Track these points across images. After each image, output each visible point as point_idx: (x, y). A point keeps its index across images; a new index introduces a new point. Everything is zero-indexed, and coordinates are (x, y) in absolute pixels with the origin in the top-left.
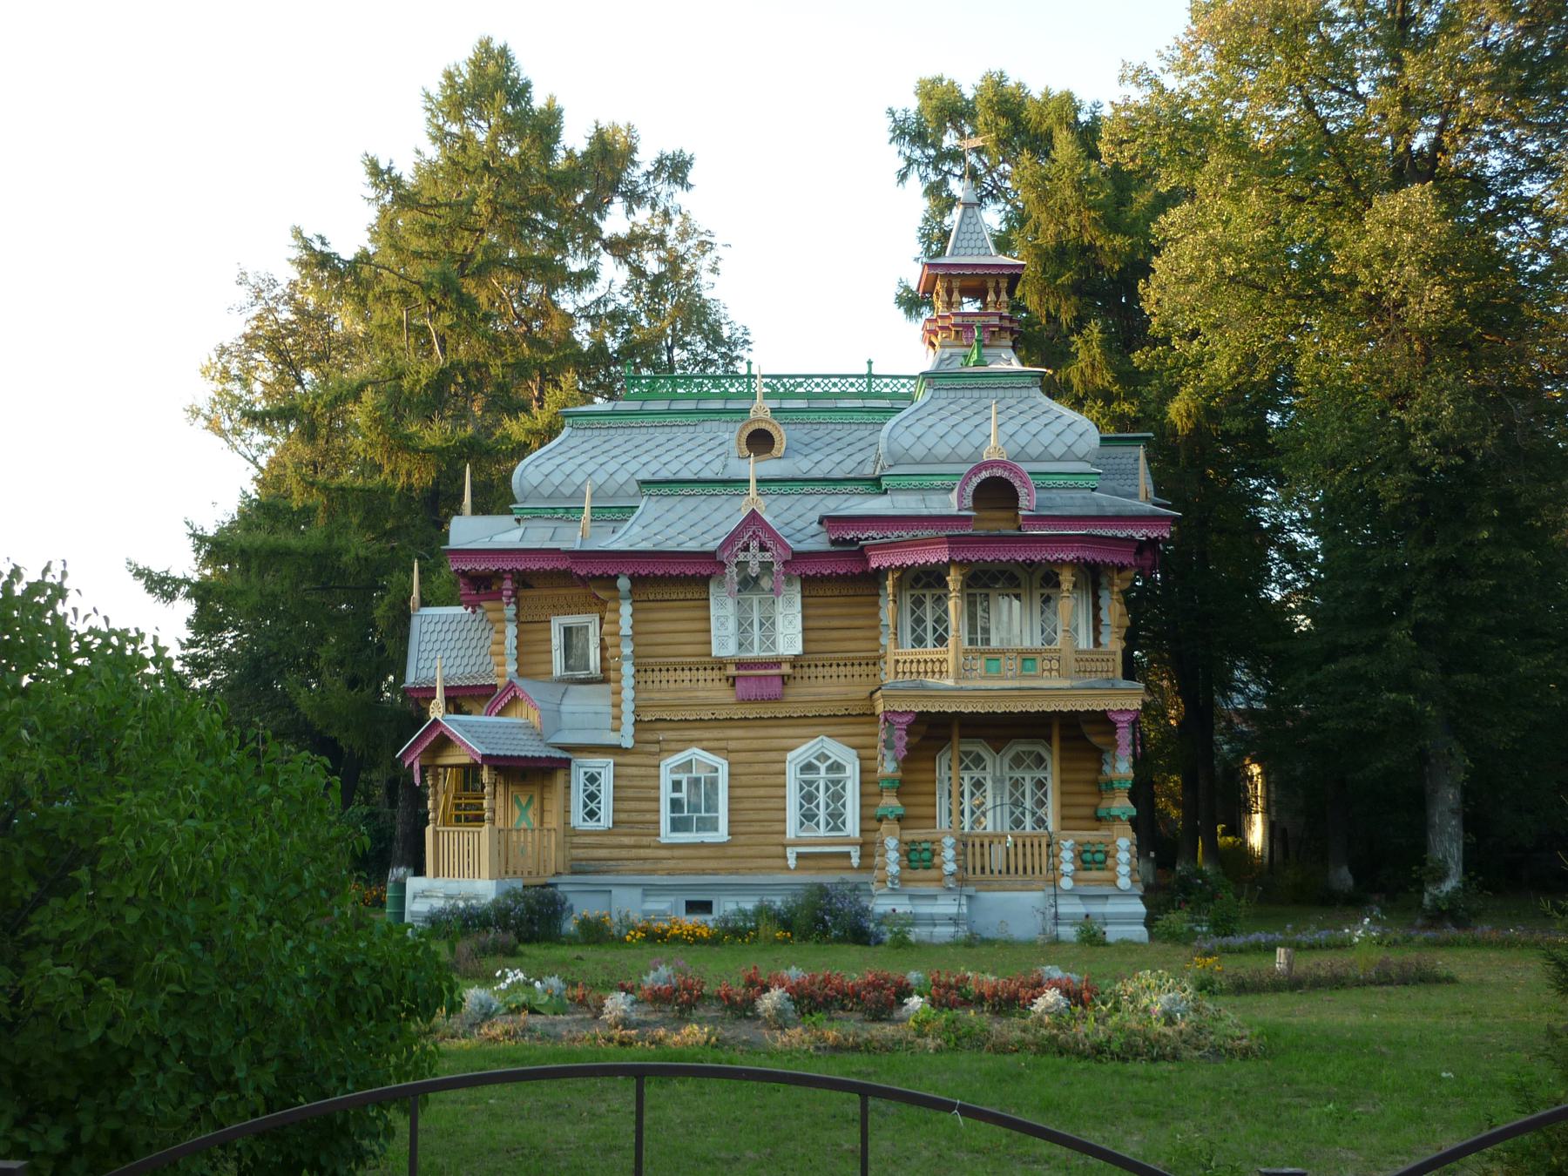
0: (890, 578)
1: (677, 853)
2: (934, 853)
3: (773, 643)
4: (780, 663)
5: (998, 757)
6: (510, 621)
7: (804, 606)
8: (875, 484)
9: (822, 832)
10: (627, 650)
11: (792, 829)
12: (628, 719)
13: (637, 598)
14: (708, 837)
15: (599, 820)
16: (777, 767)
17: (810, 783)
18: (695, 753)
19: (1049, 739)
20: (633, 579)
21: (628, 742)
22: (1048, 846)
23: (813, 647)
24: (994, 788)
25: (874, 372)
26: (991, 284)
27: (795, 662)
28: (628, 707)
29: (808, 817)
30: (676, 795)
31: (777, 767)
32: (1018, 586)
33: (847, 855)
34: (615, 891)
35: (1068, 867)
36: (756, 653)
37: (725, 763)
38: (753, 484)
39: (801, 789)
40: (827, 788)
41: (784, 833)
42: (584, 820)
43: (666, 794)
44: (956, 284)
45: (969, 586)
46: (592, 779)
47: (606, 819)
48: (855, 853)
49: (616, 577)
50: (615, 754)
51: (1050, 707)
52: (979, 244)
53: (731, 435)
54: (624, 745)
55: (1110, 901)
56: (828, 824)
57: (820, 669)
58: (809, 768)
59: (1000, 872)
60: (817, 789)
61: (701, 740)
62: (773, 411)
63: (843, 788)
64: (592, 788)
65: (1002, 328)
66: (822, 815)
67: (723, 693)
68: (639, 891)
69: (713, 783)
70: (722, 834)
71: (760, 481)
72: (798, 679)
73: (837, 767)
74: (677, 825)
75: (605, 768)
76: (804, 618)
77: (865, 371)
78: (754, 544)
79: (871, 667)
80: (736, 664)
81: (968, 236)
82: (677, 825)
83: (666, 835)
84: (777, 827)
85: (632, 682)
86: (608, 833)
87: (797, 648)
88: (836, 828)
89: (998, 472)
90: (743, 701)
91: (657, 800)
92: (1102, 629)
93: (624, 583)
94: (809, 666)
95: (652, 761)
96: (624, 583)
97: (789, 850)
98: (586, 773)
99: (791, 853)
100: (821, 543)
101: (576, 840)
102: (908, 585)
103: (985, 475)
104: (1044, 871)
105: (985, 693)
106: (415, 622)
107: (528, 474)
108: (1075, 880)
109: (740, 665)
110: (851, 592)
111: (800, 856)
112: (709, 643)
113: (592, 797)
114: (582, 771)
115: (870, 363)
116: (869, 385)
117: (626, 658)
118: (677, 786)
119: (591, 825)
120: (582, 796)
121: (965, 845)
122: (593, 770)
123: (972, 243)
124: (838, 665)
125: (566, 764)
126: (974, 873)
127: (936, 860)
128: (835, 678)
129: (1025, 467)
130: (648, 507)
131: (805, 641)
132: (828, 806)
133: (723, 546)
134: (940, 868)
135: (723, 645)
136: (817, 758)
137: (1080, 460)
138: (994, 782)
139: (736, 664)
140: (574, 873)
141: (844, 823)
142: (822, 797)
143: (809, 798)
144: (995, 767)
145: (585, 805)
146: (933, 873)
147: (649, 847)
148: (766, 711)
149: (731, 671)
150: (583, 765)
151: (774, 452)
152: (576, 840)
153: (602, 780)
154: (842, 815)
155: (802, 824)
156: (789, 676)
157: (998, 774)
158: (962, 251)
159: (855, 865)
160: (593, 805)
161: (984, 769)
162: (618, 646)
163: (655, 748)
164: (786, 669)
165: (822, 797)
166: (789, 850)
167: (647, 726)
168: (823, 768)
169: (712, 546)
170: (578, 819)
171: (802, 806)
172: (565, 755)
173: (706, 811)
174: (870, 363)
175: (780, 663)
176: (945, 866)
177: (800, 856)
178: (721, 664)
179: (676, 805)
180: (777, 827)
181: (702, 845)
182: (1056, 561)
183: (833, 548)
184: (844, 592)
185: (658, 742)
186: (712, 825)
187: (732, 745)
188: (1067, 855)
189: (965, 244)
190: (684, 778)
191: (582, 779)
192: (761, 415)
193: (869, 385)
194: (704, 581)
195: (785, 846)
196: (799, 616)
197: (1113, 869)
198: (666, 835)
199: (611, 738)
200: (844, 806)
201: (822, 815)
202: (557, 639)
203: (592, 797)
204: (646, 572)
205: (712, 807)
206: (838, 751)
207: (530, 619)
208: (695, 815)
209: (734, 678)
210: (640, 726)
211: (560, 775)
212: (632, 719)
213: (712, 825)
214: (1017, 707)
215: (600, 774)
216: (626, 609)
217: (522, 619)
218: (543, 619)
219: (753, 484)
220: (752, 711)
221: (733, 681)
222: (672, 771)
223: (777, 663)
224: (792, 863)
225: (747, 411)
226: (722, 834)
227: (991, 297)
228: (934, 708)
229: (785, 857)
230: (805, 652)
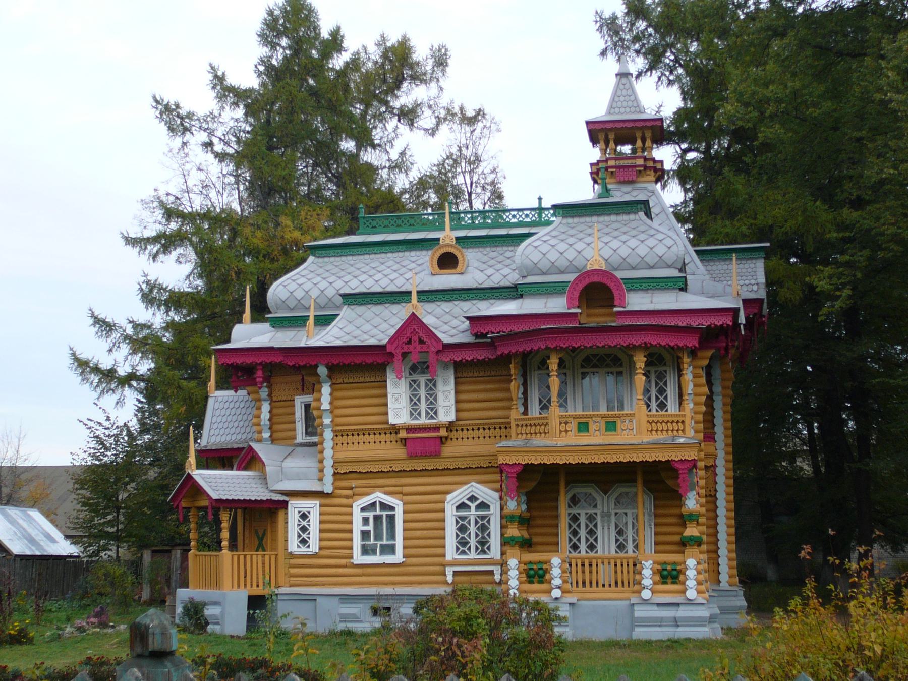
0: (513, 362)
1: (369, 570)
2: (546, 571)
3: (436, 413)
4: (439, 428)
5: (606, 498)
6: (265, 400)
7: (456, 384)
8: (514, 292)
9: (473, 555)
10: (327, 421)
11: (451, 553)
12: (329, 471)
13: (334, 381)
14: (389, 559)
15: (309, 547)
16: (439, 506)
17: (463, 518)
18: (378, 496)
19: (635, 481)
20: (332, 369)
21: (328, 489)
22: (635, 565)
23: (464, 415)
24: (602, 521)
25: (544, 205)
26: (638, 134)
27: (450, 426)
28: (328, 463)
29: (463, 543)
30: (366, 528)
31: (439, 506)
32: (621, 365)
33: (491, 573)
34: (319, 599)
35: (647, 582)
36: (423, 421)
37: (401, 503)
38: (414, 296)
39: (457, 522)
40: (476, 522)
41: (444, 556)
42: (299, 547)
43: (358, 527)
44: (612, 136)
45: (582, 366)
46: (304, 516)
47: (314, 546)
48: (497, 570)
49: (316, 366)
50: (322, 497)
51: (637, 457)
52: (630, 104)
53: (425, 259)
54: (326, 492)
55: (681, 608)
56: (477, 549)
57: (470, 432)
58: (462, 506)
59: (610, 585)
60: (469, 522)
61: (383, 487)
62: (457, 239)
63: (489, 521)
64: (304, 523)
65: (646, 168)
66: (473, 542)
67: (400, 452)
68: (337, 598)
69: (391, 518)
70: (398, 557)
71: (418, 292)
72: (454, 440)
73: (483, 506)
74: (366, 551)
75: (313, 506)
76: (457, 392)
77: (536, 205)
78: (415, 338)
79: (503, 430)
80: (407, 429)
81: (622, 99)
82: (366, 551)
83: (358, 558)
84: (439, 551)
85: (331, 444)
86: (315, 556)
87: (452, 417)
88: (484, 552)
89: (596, 279)
90: (412, 456)
91: (351, 531)
92: (685, 397)
93: (322, 371)
94: (462, 430)
95: (349, 501)
96: (322, 371)
97: (447, 569)
98: (299, 512)
99: (449, 571)
100: (467, 338)
101: (293, 561)
102: (536, 367)
103: (587, 281)
104: (631, 583)
105: (618, 447)
106: (211, 401)
107: (278, 291)
108: (653, 592)
109: (410, 429)
110: (493, 373)
111: (455, 573)
112: (387, 414)
113: (304, 529)
114: (297, 510)
115: (540, 199)
116: (540, 216)
117: (327, 426)
118: (366, 521)
119: (303, 550)
120: (297, 529)
121: (570, 565)
122: (305, 510)
123: (625, 104)
124: (484, 429)
125: (284, 505)
126: (577, 586)
127: (547, 577)
128: (482, 438)
129: (620, 275)
130: (346, 312)
131: (457, 410)
132: (477, 535)
133: (393, 340)
134: (550, 582)
135: (397, 415)
136: (469, 499)
137: (669, 267)
138: (602, 517)
139: (407, 429)
140: (290, 586)
141: (489, 548)
142: (473, 529)
143: (462, 529)
144: (604, 504)
145: (299, 536)
146: (544, 586)
147: (345, 566)
148: (429, 464)
149: (403, 434)
150: (295, 507)
151: (458, 269)
152: (293, 561)
153: (311, 517)
154: (487, 542)
155: (458, 549)
156: (447, 438)
157: (606, 510)
158: (617, 110)
159: (498, 580)
160: (304, 536)
161: (595, 506)
162: (321, 417)
163: (349, 492)
164: (443, 433)
165: (473, 529)
166: (447, 569)
167: (342, 477)
168: (473, 506)
169: (384, 342)
170: (293, 546)
171: (457, 536)
172: (286, 499)
173: (388, 540)
174: (540, 199)
175: (439, 428)
176: (553, 581)
177: (455, 573)
178: (395, 429)
179: (365, 535)
180: (439, 551)
181: (384, 565)
182: (627, 346)
183: (477, 341)
184: (488, 374)
185: (351, 488)
186: (390, 550)
187: (406, 490)
188: (647, 572)
189: (619, 104)
190: (370, 515)
191: (297, 516)
192: (448, 241)
193: (540, 216)
194: (381, 368)
195: (444, 566)
196: (453, 392)
197: (684, 583)
198: (358, 558)
199: (315, 487)
200: (489, 535)
201: (473, 542)
202: (299, 413)
203: (304, 529)
204: (337, 361)
205: (392, 536)
206: (486, 493)
207: (280, 398)
208: (379, 543)
209: (405, 439)
210: (338, 476)
211: (281, 514)
212: (331, 471)
213: (390, 550)
214: (599, 459)
215: (309, 512)
216: (326, 390)
217: (275, 399)
218: (289, 398)
219: (414, 296)
220: (419, 464)
221: (404, 442)
222: (363, 510)
223: (436, 428)
224: (450, 578)
225: (438, 239)
226: (398, 557)
227: (639, 143)
228: (535, 460)
229: (445, 575)
230: (458, 420)
